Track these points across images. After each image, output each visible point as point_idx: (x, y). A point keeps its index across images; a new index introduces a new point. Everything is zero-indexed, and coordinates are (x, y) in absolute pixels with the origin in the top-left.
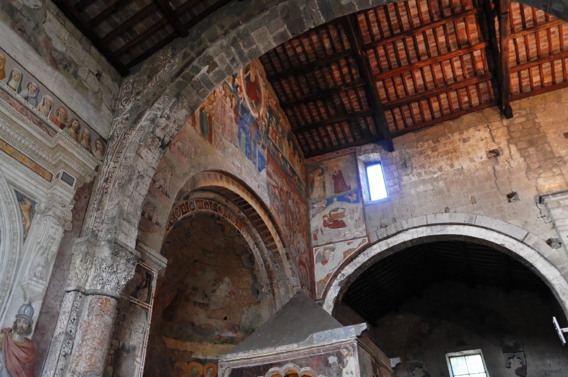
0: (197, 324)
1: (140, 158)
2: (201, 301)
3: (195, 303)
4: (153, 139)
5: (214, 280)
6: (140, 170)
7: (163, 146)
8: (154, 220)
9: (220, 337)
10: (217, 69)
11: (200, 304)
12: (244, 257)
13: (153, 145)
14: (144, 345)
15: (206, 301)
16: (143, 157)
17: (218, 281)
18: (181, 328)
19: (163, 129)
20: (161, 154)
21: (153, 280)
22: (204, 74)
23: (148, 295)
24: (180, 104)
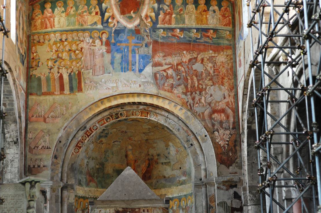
0: (167, 176)
1: (8, 155)
3: (162, 163)
4: (9, 144)
5: (166, 147)
7: (15, 143)
8: (42, 166)
9: (179, 180)
10: (7, 104)
11: (165, 163)
12: (166, 129)
15: (168, 161)
17: (167, 146)
18: (158, 182)
19: (10, 137)
20: (16, 146)
22: (5, 109)
23: (45, 200)
24: (8, 124)
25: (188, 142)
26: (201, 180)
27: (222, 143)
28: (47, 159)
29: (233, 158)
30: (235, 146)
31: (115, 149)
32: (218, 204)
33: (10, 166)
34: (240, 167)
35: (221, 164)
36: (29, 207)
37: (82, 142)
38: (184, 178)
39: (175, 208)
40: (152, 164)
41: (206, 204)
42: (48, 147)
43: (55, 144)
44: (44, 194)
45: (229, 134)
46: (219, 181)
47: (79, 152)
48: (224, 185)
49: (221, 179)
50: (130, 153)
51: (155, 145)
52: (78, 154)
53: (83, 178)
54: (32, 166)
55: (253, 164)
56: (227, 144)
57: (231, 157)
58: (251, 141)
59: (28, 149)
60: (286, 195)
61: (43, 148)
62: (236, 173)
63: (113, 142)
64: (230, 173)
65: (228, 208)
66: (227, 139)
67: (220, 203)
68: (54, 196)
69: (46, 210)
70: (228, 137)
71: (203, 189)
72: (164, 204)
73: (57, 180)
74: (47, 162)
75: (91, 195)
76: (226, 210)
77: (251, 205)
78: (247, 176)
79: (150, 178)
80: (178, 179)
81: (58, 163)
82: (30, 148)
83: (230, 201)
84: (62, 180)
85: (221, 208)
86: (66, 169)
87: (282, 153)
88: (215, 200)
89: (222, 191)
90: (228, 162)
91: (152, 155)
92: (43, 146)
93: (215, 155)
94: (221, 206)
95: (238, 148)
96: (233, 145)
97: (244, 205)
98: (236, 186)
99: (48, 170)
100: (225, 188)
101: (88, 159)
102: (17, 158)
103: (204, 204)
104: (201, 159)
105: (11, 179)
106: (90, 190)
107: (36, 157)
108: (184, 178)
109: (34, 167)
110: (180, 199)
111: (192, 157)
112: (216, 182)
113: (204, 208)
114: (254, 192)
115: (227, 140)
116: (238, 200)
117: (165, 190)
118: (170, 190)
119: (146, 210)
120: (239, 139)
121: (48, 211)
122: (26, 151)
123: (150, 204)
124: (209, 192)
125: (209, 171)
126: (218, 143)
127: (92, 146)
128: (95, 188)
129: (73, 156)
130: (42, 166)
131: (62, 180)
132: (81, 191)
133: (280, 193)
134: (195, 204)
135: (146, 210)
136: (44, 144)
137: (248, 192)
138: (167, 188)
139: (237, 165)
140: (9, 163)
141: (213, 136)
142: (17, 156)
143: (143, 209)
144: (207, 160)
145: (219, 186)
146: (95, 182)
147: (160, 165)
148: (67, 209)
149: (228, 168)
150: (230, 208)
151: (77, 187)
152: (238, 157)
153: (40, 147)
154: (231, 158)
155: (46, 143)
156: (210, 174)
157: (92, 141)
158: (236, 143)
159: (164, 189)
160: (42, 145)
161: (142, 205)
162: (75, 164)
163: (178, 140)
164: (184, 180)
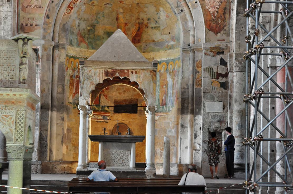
0: (156, 40)
2: (155, 26)
3: (152, 28)
5: (156, 11)
6: (4, 16)
8: (34, 25)
9: (168, 45)
11: (155, 27)
13: (3, 3)
14: (39, 78)
15: (158, 25)
16: (2, 10)
17: (158, 11)
18: (147, 45)
20: (9, 4)
21: (38, 51)
23: (37, 58)
25: (178, 8)
26: (189, 45)
27: (211, 10)
28: (39, 18)
29: (221, 26)
30: (224, 13)
31: (106, 11)
32: (204, 69)
33: (3, 23)
34: (228, 34)
35: (209, 30)
36: (22, 64)
37: (74, 3)
38: (172, 43)
39: (162, 71)
40: (142, 27)
41: (193, 69)
42: (40, 6)
43: (48, 4)
44: (36, 52)
45: (220, 2)
46: (207, 47)
47: (71, 13)
48: (211, 51)
49: (209, 45)
50: (120, 16)
51: (146, 9)
52: (70, 14)
53: (74, 38)
54: (24, 25)
55: (241, 32)
56: (217, 12)
57: (219, 25)
58: (240, 9)
59: (21, 7)
60: (271, 63)
61: (35, 7)
62: (223, 40)
63: (105, 5)
64: (218, 40)
65: (214, 74)
66: (217, 7)
67: (206, 68)
68: (46, 55)
69: (38, 68)
70: (218, 4)
71: (191, 54)
72: (152, 67)
73: (49, 39)
74: (39, 21)
75: (82, 55)
76: (212, 75)
77: (236, 72)
78: (234, 44)
79: (139, 41)
80: (166, 44)
81: (50, 23)
82: (23, 6)
83: (216, 67)
84: (53, 39)
85: (207, 73)
86: (58, 28)
87: (270, 22)
88: (202, 65)
89: (209, 57)
90: (217, 29)
91: (143, 19)
92: (36, 6)
93: (204, 21)
94: (207, 71)
95: (227, 16)
96: (223, 12)
97: (230, 72)
98: (223, 53)
99: (40, 29)
100: (212, 54)
101: (80, 20)
102: (10, 16)
103: (191, 68)
104: (190, 25)
105: (4, 36)
106: (80, 51)
107: (29, 16)
108: (172, 43)
109: (27, 25)
110: (168, 63)
111: (182, 23)
112: (203, 48)
113: (190, 72)
114: (240, 59)
115: (217, 7)
116: (224, 66)
117: (154, 54)
118: (158, 54)
119: (134, 72)
120: (229, 7)
121: (40, 69)
122: (19, 9)
123: (138, 66)
124: (196, 56)
125: (197, 37)
126: (208, 10)
127: (84, 8)
128: (86, 49)
129: (64, 16)
130: (35, 25)
131: (53, 39)
132: (72, 51)
133: (266, 61)
134: (182, 68)
135: (135, 72)
136: (36, 3)
137: (234, 59)
138: (156, 52)
139: (225, 32)
140: (3, 20)
141: (203, 2)
142: (10, 14)
143: (132, 70)
144: (196, 26)
145: (206, 52)
146: (86, 43)
147: (150, 30)
148: (58, 67)
149: (217, 34)
150: (216, 74)
151: (68, 47)
152: (227, 25)
153: (33, 6)
154: (220, 26)
155: (39, 3)
156: (198, 40)
157: (84, 3)
158: (226, 11)
159: (153, 53)
160: (35, 4)
161: (131, 67)
162: (67, 24)
163: (168, 6)
164: (173, 45)
